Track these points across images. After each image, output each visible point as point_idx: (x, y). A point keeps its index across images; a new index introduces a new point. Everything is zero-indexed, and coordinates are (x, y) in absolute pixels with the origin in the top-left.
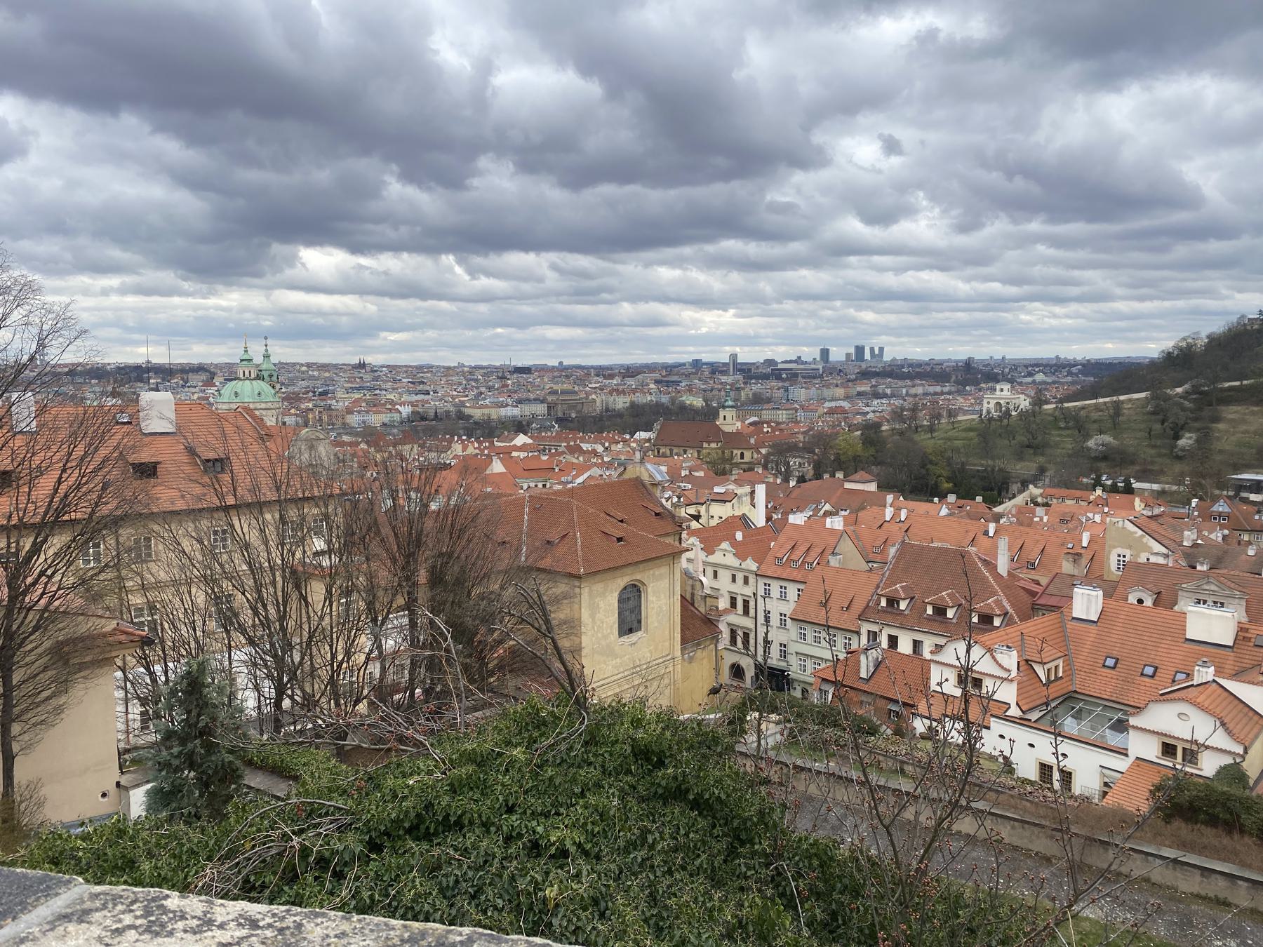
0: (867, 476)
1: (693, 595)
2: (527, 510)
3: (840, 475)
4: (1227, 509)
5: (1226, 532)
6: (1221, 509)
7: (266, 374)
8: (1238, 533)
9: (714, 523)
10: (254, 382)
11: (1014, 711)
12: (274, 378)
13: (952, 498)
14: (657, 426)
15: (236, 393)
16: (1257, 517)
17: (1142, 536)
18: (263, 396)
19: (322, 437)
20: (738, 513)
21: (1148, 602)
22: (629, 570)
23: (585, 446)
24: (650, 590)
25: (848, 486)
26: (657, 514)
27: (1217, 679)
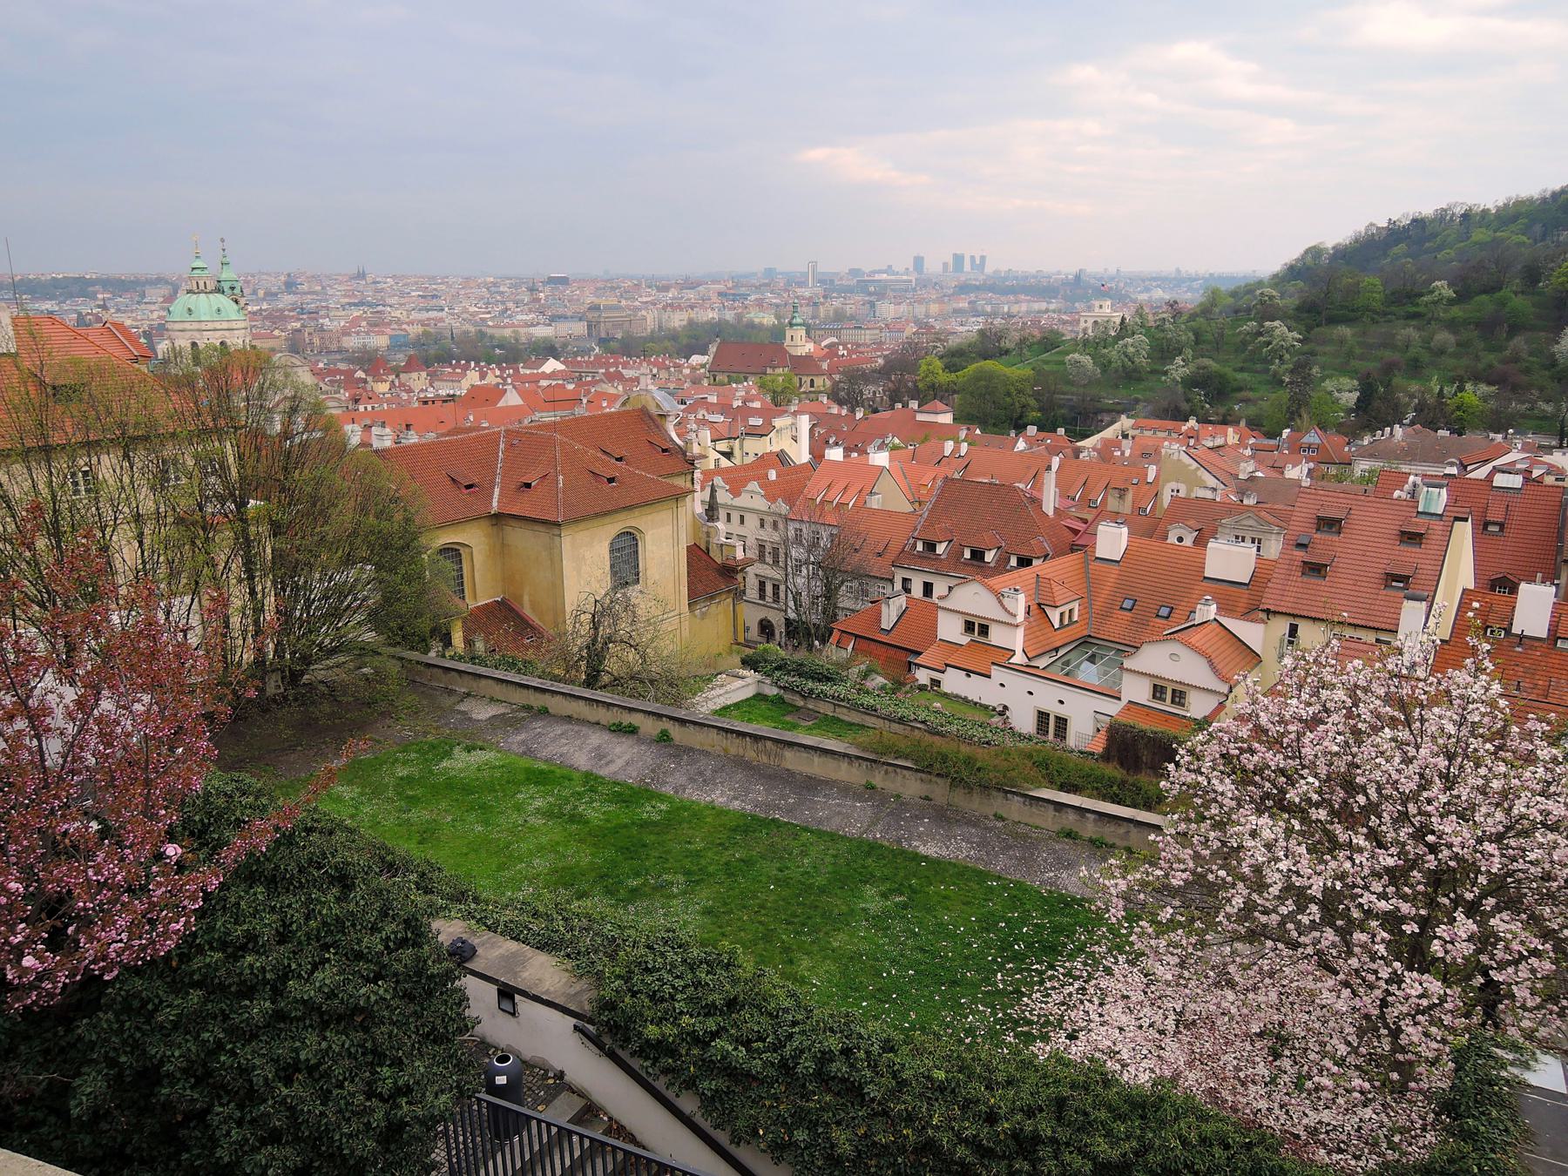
0: (940, 405)
1: (708, 542)
2: (502, 446)
3: (914, 405)
4: (1318, 441)
5: (1311, 465)
6: (1312, 440)
7: (226, 286)
8: (1322, 466)
9: (749, 459)
10: (211, 296)
11: (1019, 658)
12: (237, 291)
13: (1032, 430)
14: (713, 349)
15: (189, 310)
16: (1346, 449)
17: (1198, 469)
18: (223, 314)
19: (299, 363)
20: (776, 448)
21: (1188, 542)
22: (621, 516)
23: (628, 373)
24: (648, 538)
25: (920, 417)
26: (664, 451)
27: (1223, 620)
